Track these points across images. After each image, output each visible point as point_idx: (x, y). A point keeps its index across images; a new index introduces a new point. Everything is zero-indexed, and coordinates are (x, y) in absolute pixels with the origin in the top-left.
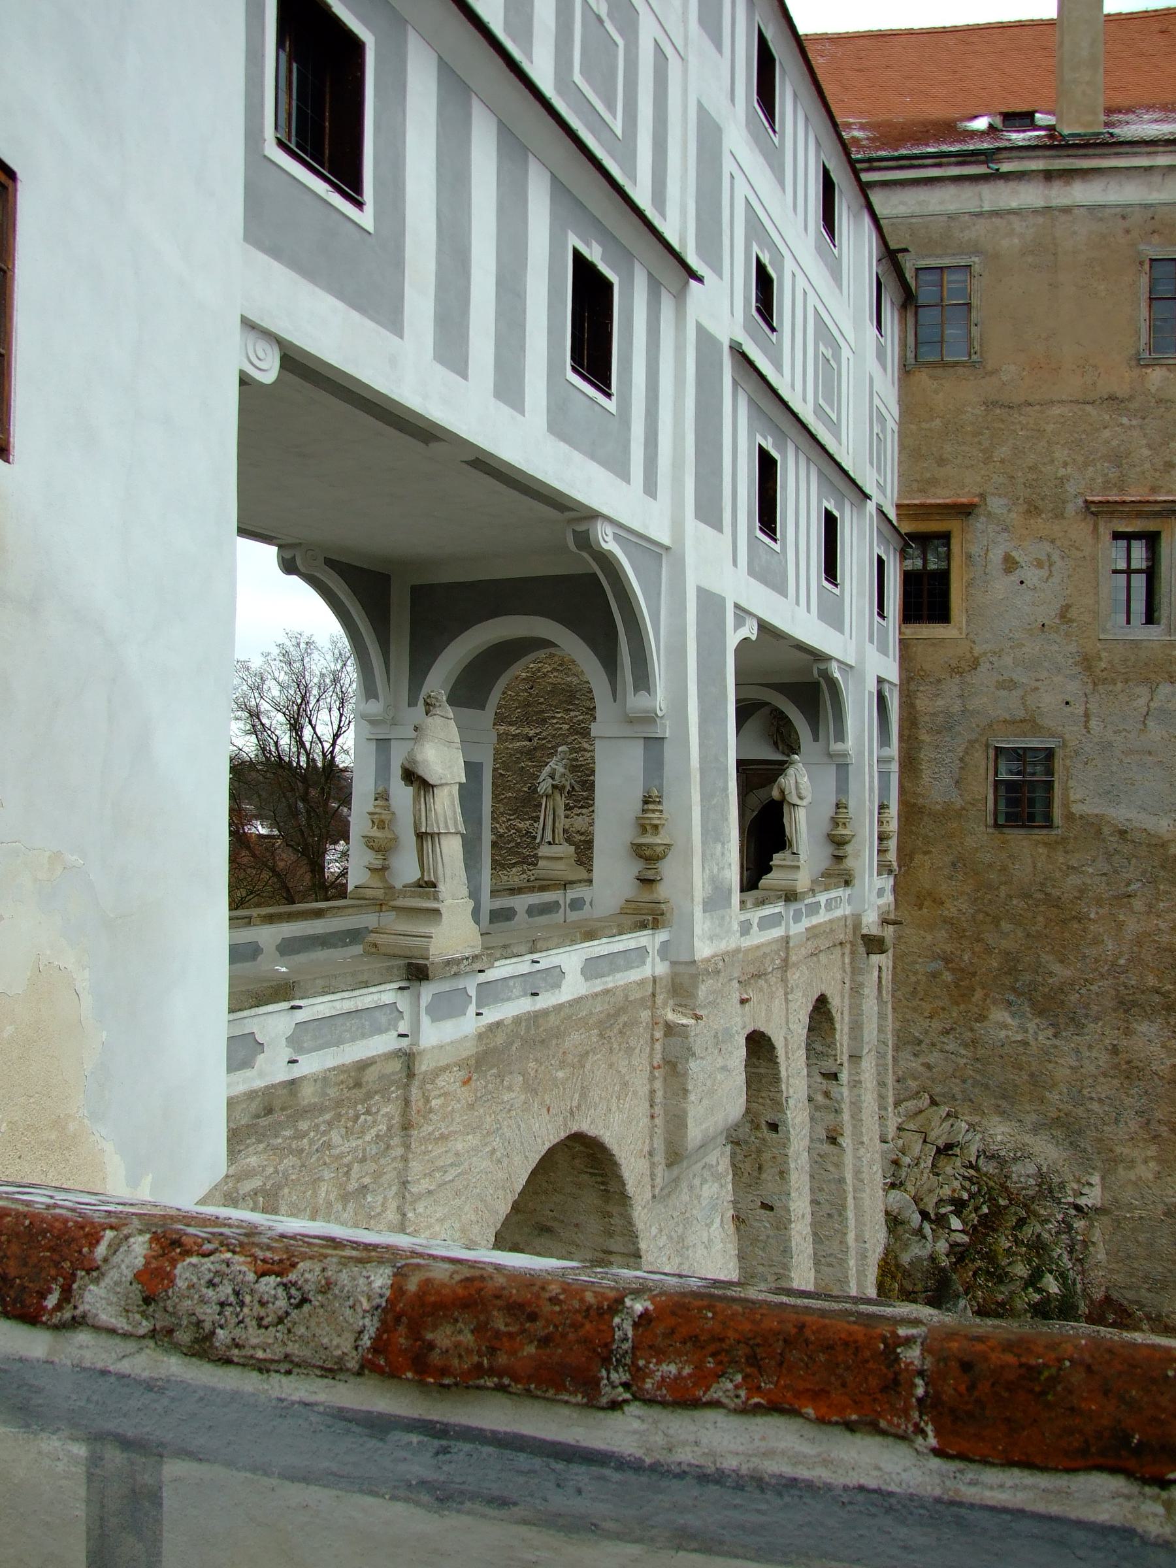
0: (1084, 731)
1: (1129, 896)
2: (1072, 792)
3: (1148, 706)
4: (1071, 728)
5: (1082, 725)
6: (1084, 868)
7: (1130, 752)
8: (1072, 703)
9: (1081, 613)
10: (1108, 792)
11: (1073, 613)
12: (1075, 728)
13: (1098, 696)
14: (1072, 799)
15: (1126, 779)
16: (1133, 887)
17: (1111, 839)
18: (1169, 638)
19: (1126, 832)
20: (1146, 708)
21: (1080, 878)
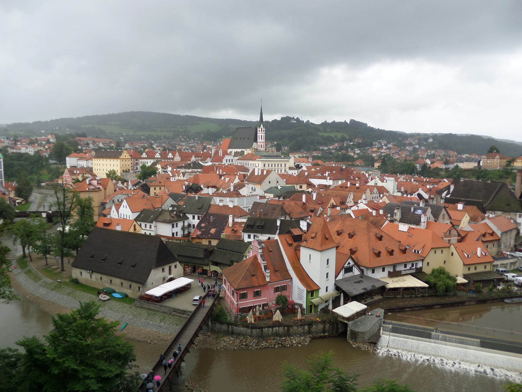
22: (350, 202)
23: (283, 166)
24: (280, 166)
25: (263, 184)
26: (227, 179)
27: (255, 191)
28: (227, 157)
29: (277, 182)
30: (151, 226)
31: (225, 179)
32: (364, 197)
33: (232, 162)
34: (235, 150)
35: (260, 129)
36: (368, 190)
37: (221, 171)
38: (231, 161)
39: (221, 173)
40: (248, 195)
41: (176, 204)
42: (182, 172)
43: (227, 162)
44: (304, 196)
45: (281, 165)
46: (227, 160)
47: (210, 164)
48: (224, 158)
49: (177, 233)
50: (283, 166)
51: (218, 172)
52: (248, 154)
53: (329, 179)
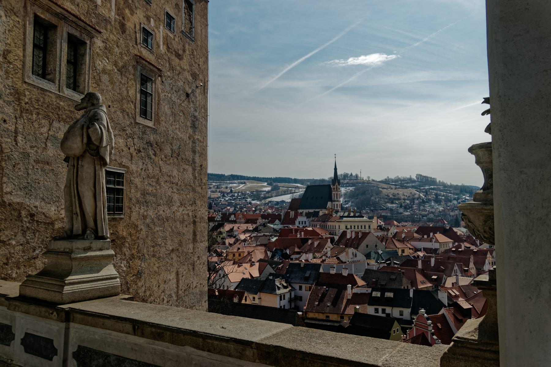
0: (14, 143)
1: (34, 258)
2: (5, 185)
3: (48, 133)
4: (6, 140)
5: (13, 138)
6: (10, 242)
7: (37, 162)
8: (8, 122)
9: (16, 60)
10: (25, 188)
11: (11, 57)
12: (9, 140)
13: (22, 121)
14: (5, 191)
15: (35, 179)
16: (37, 252)
17: (26, 219)
18: (59, 94)
19: (34, 215)
20: (47, 135)
21: (7, 249)
22: (472, 269)
23: (367, 227)
24: (363, 227)
25: (360, 248)
26: (316, 243)
27: (356, 256)
28: (300, 219)
29: (376, 246)
30: (254, 298)
31: (312, 244)
32: (487, 261)
33: (305, 224)
34: (307, 211)
35: (335, 187)
36: (489, 253)
37: (303, 233)
38: (304, 223)
39: (303, 237)
40: (348, 261)
41: (275, 272)
42: (254, 236)
43: (299, 224)
44: (420, 262)
45: (365, 226)
46: (299, 222)
47: (280, 226)
48: (297, 219)
49: (284, 306)
50: (367, 227)
51: (298, 236)
52: (325, 215)
53: (435, 242)
